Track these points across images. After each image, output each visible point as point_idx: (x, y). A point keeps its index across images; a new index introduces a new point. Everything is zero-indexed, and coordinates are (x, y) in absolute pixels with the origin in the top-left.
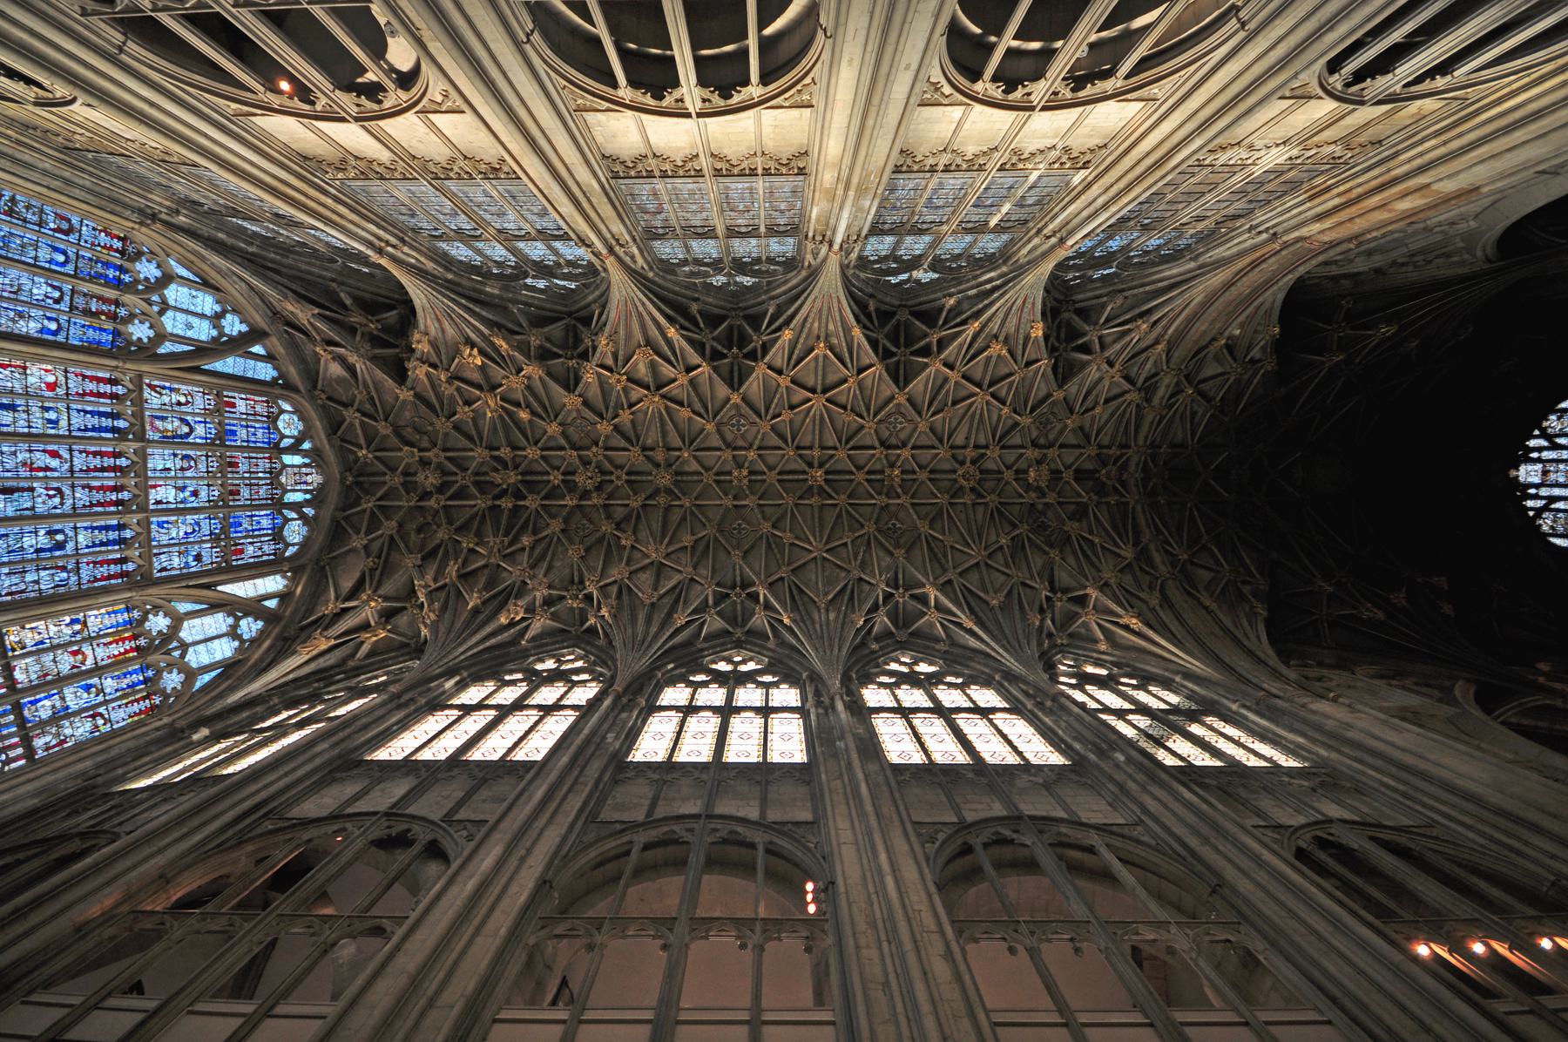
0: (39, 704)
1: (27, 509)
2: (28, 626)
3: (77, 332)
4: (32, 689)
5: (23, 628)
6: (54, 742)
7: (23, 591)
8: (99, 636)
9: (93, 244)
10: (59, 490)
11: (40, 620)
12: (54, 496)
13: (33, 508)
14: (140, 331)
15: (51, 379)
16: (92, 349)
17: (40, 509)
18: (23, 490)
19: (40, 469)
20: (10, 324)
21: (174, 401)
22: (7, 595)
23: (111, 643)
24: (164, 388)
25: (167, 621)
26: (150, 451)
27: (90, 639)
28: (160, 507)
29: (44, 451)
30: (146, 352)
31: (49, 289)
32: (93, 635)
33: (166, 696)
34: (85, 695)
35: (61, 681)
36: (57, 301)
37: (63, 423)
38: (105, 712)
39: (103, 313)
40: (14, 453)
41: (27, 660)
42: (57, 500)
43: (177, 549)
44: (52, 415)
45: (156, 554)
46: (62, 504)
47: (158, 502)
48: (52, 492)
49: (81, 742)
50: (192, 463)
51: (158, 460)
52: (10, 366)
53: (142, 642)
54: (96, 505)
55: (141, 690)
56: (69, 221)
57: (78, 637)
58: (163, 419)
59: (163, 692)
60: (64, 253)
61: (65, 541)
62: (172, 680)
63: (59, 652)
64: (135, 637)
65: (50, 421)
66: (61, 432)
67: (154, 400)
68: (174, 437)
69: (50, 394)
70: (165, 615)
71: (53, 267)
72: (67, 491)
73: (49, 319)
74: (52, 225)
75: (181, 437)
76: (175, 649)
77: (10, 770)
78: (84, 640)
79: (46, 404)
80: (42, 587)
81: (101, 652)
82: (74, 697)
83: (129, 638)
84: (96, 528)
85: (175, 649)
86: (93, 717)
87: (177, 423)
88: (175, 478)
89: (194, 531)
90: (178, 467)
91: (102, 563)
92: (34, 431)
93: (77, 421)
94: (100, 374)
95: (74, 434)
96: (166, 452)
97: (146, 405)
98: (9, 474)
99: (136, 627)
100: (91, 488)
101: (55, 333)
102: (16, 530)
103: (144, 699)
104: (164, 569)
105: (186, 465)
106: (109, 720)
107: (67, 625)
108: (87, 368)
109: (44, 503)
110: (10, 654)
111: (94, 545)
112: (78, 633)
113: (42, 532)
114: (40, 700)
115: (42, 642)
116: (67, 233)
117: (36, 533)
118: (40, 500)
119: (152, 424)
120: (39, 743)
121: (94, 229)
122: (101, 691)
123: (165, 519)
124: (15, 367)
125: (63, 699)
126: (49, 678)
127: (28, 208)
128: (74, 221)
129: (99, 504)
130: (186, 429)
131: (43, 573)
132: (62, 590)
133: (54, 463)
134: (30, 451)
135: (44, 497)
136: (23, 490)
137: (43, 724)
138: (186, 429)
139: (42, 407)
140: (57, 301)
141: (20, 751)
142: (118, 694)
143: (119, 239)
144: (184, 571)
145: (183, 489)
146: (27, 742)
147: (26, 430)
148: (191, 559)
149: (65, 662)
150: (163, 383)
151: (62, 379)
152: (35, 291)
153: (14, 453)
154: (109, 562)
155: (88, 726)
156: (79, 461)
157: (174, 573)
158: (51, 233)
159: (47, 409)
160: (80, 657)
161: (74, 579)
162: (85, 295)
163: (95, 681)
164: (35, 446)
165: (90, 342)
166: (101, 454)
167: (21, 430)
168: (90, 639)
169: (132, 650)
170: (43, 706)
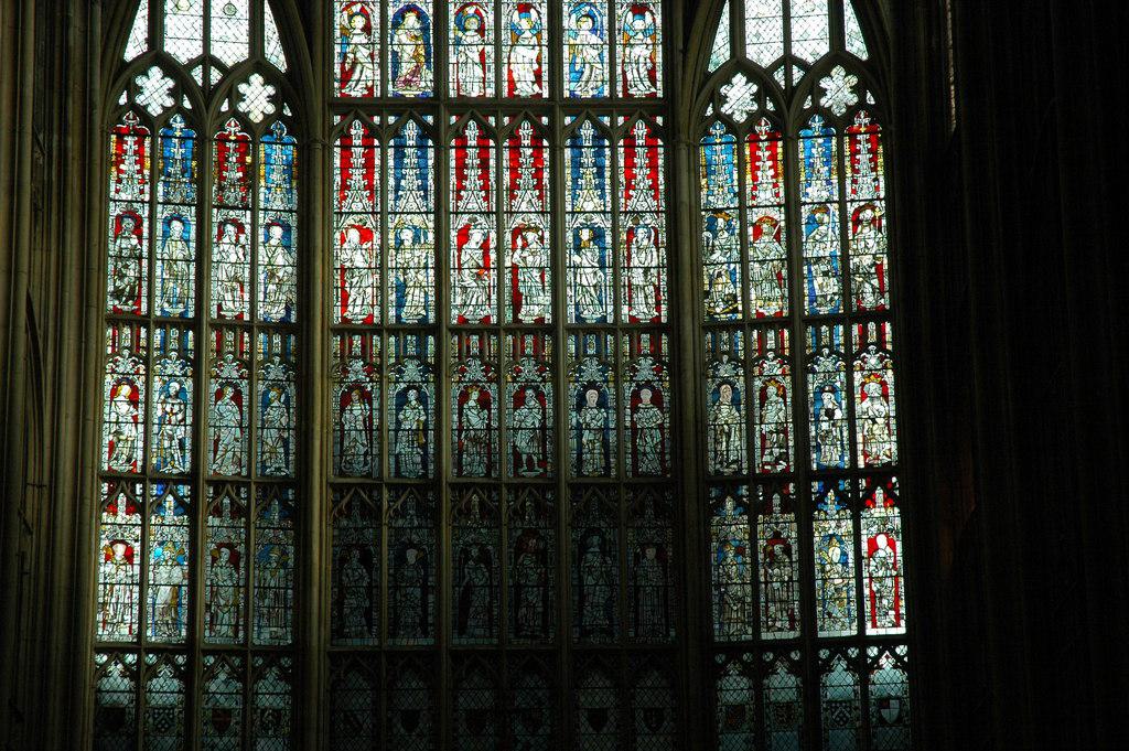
0: (818, 292)
1: (542, 277)
2: (707, 288)
3: (275, 194)
4: (795, 297)
5: (707, 294)
6: (875, 282)
7: (657, 289)
8: (741, 195)
9: (142, 182)
10: (517, 232)
11: (700, 275)
12: (524, 239)
13: (542, 269)
14: (257, 98)
15: (354, 235)
16: (307, 178)
17: (543, 259)
18: (515, 281)
19: (486, 256)
20: (285, 288)
21: (363, 39)
22: (659, 310)
23: (755, 178)
24: (344, 56)
25: (739, 79)
26: (452, 94)
27: (742, 208)
28: (545, 77)
29: (460, 249)
30: (288, 88)
31: (226, 240)
32: (736, 203)
33: (862, 104)
34: (823, 228)
35: (794, 261)
36: (240, 228)
37: (417, 220)
38: (856, 205)
39: (241, 160)
40: (464, 289)
41: (753, 297)
42: (531, 236)
43: (619, 49)
44: (407, 235)
45: (625, 89)
46: (536, 229)
47: (538, 74)
48: (519, 242)
49: (889, 246)
50: (471, 10)
51: (469, 79)
52: (343, 288)
53: (763, 128)
54: (540, 180)
55: (840, 145)
56: (119, 219)
57: (736, 224)
58: (397, 64)
59: (852, 111)
60: (168, 222)
61: (591, 228)
62: (838, 90)
63: (751, 253)
64: (755, 140)
65: (416, 239)
66: (431, 225)
67: (365, 79)
68: (427, 44)
69: (377, 236)
70: (728, 82)
71: (193, 235)
72: (518, 221)
73: (268, 238)
74: (134, 241)
75: (425, 29)
76: (788, 75)
77: (893, 343)
78: (742, 217)
79: (392, 243)
80: (654, 264)
81: (765, 195)
82: (822, 243)
83: (755, 148)
84: (575, 181)
85: (788, 75)
86: (857, 222)
87: (402, 36)
88: (498, 44)
89: (589, 15)
90: (477, 38)
91: (630, 177)
92: (431, 262)
93: (411, 201)
94: (337, 162)
95: (431, 205)
96: (453, 59)
97: (377, 93)
98: (494, 297)
99: (741, 133)
100: (514, 186)
101: (286, 228)
102: (570, 292)
103: (854, 142)
104: (651, 75)
105: (473, 24)
106: (870, 205)
107: (715, 237)
108: (331, 181)
109: (533, 254)
110: (740, 316)
111: (601, 187)
112: (728, 223)
113: (576, 259)
114: (812, 289)
115: (733, 273)
116: (138, 221)
117: (576, 267)
118: (530, 259)
119: (408, 82)
120: (869, 300)
121: (119, 181)
122: (823, 206)
123: (566, 69)
124: (344, 282)
125: (818, 260)
126: (784, 272)
127: (122, 277)
128: (118, 212)
129: (538, 175)
130: (411, 19)
131: (635, 262)
132: (663, 238)
133: (476, 237)
134: (460, 268)
135: (525, 254)
136: (515, 281)
137: (846, 292)
138: (411, 19)
139: (397, 250)
140: (240, 228)
141: (872, 326)
142: (835, 179)
143: (120, 141)
144: (659, 37)
145: (516, 33)
146: (863, 316)
147: (431, 272)
148: (639, 24)
149: (768, 248)
150: (337, 60)
151: (351, 220)
152: (233, 258)
153: (464, 289)
154: (630, 165)
155: (868, 232)
156: (473, 201)
157: (659, 60)
158: (145, 243)
159: (400, 243)
160: (765, 227)
161: (649, 219)
162: (221, 188)
163: (805, 211)
164: (453, 262)
165: (291, 177)
166: (461, 166)
167: (431, 279)
168: (742, 208)
169: (772, 148)
170: (821, 286)
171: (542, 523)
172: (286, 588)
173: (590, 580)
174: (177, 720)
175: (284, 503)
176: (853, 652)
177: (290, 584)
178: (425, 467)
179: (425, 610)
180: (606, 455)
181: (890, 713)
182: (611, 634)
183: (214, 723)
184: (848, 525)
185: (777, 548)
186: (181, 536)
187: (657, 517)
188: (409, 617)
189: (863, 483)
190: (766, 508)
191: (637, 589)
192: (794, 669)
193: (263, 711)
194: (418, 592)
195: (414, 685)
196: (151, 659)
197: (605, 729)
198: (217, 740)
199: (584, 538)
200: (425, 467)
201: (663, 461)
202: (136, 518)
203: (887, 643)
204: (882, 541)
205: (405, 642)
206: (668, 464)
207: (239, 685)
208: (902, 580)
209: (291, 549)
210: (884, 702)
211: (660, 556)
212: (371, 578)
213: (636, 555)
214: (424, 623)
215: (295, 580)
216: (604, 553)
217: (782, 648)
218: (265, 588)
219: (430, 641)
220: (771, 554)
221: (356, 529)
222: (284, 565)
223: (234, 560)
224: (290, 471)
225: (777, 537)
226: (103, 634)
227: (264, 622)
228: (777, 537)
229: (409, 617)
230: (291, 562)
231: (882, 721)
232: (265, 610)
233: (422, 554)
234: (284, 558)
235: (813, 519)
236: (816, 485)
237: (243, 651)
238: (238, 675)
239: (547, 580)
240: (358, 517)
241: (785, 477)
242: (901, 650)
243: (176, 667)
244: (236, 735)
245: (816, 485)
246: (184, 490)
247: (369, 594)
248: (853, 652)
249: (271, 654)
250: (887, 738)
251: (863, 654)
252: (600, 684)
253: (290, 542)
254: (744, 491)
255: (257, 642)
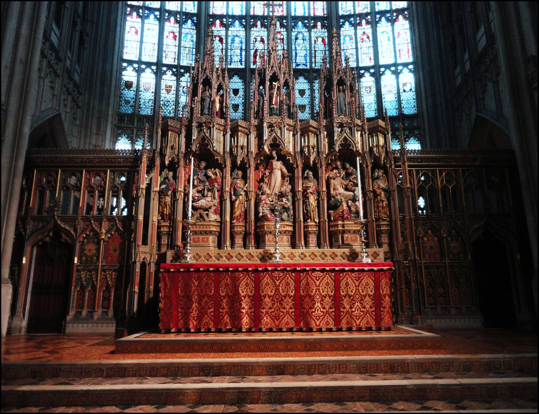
171: (282, 30)
172: (193, 48)
173: (298, 48)
174: (152, 88)
175: (193, 21)
176: (393, 68)
177: (194, 47)
178: (242, 11)
179: (241, 57)
180: (304, 9)
181: (407, 88)
182: (306, 65)
183: (166, 90)
184: (390, 28)
185: (365, 37)
186: (157, 28)
187: (322, 29)
188: (236, 59)
189: (395, 14)
190: (360, 24)
191: (315, 51)
192: (372, 75)
193: (184, 87)
194: (239, 51)
195: (237, 81)
196: (143, 66)
197: (304, 96)
198: (166, 95)
199: (297, 35)
200: (242, 11)
201: (324, 11)
202: (140, 20)
203: (405, 65)
204: (402, 33)
205: (233, 66)
206: (326, 13)
207: (175, 78)
208: (410, 45)
209: (195, 36)
210: (405, 85)
211: (323, 41)
212: (222, 46)
213: (315, 41)
214: (241, 61)
215: (196, 46)
216: (304, 40)
217: (367, 69)
218: (185, 47)
219: (243, 67)
220: (362, 39)
221: (218, 31)
222: (192, 41)
223: (175, 37)
224: (195, 11)
225: (364, 33)
226: (125, 57)
227: (185, 58)
228: (364, 33)
229: (236, 59)
230: (195, 40)
231: (404, 91)
232: (185, 55)
233: (240, 39)
234: (192, 39)
235: (376, 26)
236: (378, 16)
237: (178, 67)
238: (174, 74)
239: (284, 48)
240: (219, 27)
241: (367, 14)
242: (411, 67)
243: (152, 70)
244: (173, 94)
245: (378, 16)
246: (157, 13)
247: (222, 52)
248: (393, 68)
249: (187, 69)
250: (406, 96)
251: (397, 69)
252: (303, 82)
253: (195, 33)
254: (352, 19)
255: (181, 64)
